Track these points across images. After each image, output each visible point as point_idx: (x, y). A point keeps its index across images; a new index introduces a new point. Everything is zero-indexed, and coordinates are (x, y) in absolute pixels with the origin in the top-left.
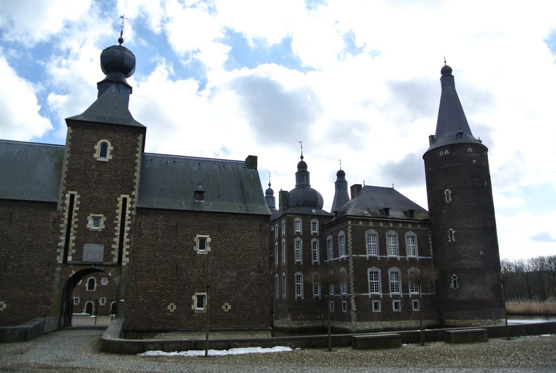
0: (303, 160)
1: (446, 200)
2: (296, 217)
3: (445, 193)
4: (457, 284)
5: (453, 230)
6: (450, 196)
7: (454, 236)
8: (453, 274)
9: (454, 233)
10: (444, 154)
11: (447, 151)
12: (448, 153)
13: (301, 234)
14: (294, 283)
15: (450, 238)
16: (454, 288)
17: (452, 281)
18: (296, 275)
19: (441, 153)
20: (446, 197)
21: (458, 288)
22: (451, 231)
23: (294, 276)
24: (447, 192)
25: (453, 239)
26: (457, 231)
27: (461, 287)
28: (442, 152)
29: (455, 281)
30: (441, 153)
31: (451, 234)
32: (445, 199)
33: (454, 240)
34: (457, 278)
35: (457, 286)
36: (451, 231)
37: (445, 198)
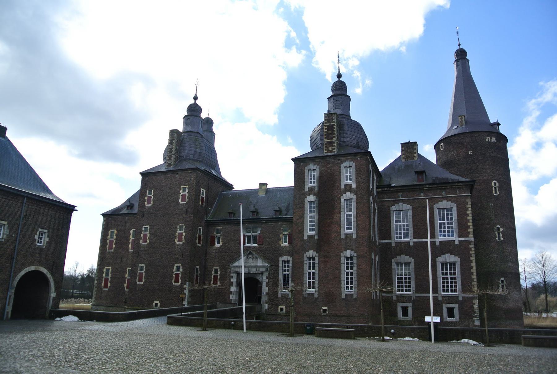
1: (494, 192)
3: (493, 184)
6: (497, 189)
7: (503, 235)
9: (501, 231)
10: (491, 140)
11: (494, 138)
15: (497, 236)
19: (488, 139)
20: (493, 188)
22: (499, 228)
25: (501, 237)
30: (488, 139)
31: (499, 232)
32: (492, 191)
33: (502, 239)
36: (499, 228)
37: (492, 189)
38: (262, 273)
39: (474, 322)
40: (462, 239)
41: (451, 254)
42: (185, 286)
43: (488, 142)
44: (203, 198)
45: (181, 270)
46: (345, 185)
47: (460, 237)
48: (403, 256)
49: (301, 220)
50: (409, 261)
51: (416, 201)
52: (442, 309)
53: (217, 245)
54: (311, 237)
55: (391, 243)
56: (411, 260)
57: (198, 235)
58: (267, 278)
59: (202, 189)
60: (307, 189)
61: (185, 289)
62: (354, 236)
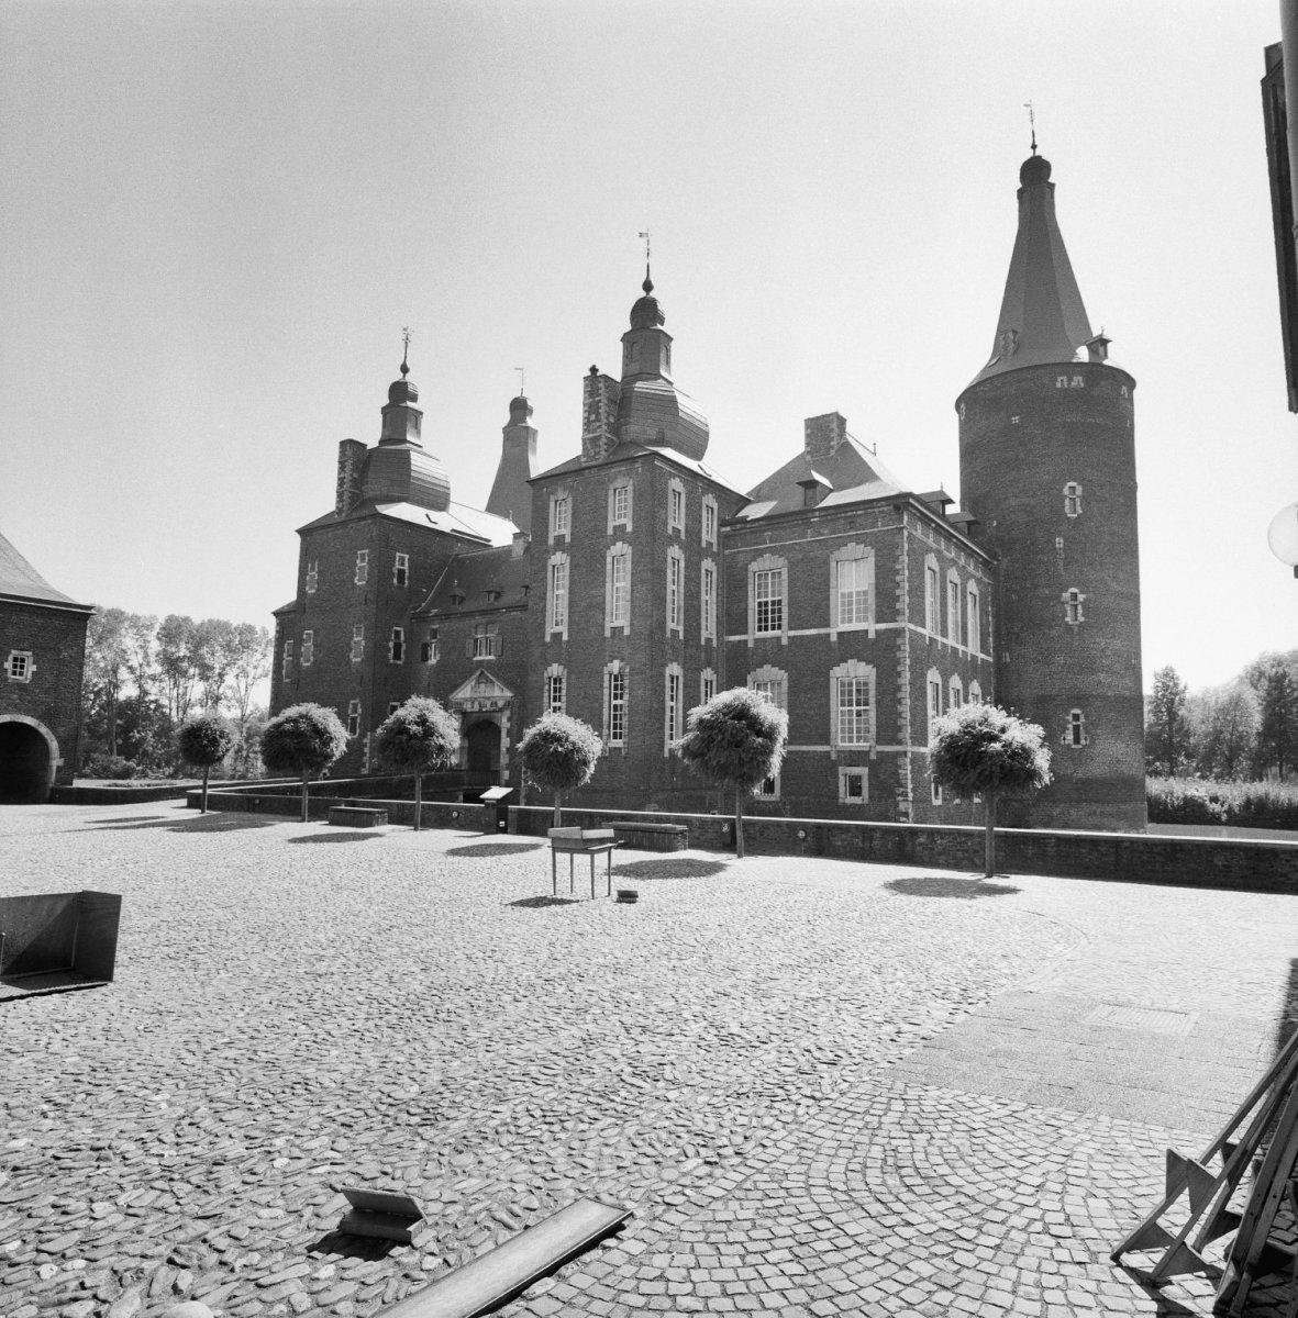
0: (652, 294)
1: (1067, 510)
2: (674, 476)
3: (1066, 491)
4: (1083, 735)
5: (1082, 592)
8: (1073, 707)
11: (1080, 378)
12: (1082, 385)
13: (683, 536)
14: (663, 701)
16: (1073, 746)
17: (1070, 726)
18: (668, 672)
21: (1084, 746)
23: (662, 675)
24: (1073, 488)
26: (1091, 595)
27: (1093, 742)
28: (1065, 378)
29: (1076, 728)
33: (1082, 619)
34: (1082, 719)
35: (1083, 742)
36: (1074, 596)
38: (501, 710)
39: (897, 805)
40: (883, 626)
41: (859, 660)
42: (365, 741)
43: (1063, 390)
44: (401, 572)
45: (360, 711)
46: (615, 527)
47: (878, 621)
48: (767, 667)
49: (541, 605)
50: (779, 678)
51: (797, 547)
52: (837, 777)
53: (433, 661)
54: (557, 636)
55: (746, 641)
56: (782, 675)
57: (391, 644)
58: (509, 719)
59: (398, 554)
60: (551, 541)
61: (365, 745)
62: (627, 632)
